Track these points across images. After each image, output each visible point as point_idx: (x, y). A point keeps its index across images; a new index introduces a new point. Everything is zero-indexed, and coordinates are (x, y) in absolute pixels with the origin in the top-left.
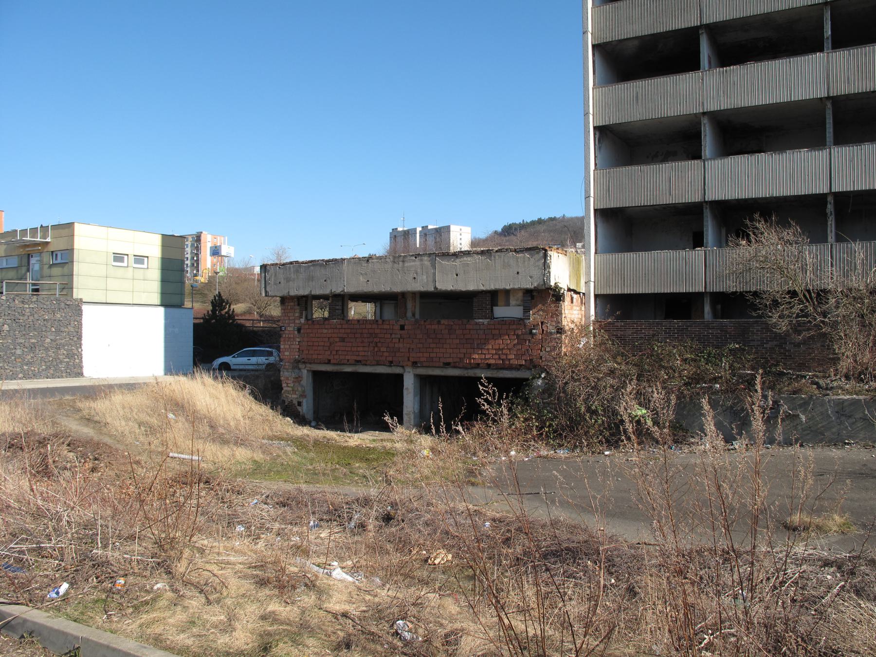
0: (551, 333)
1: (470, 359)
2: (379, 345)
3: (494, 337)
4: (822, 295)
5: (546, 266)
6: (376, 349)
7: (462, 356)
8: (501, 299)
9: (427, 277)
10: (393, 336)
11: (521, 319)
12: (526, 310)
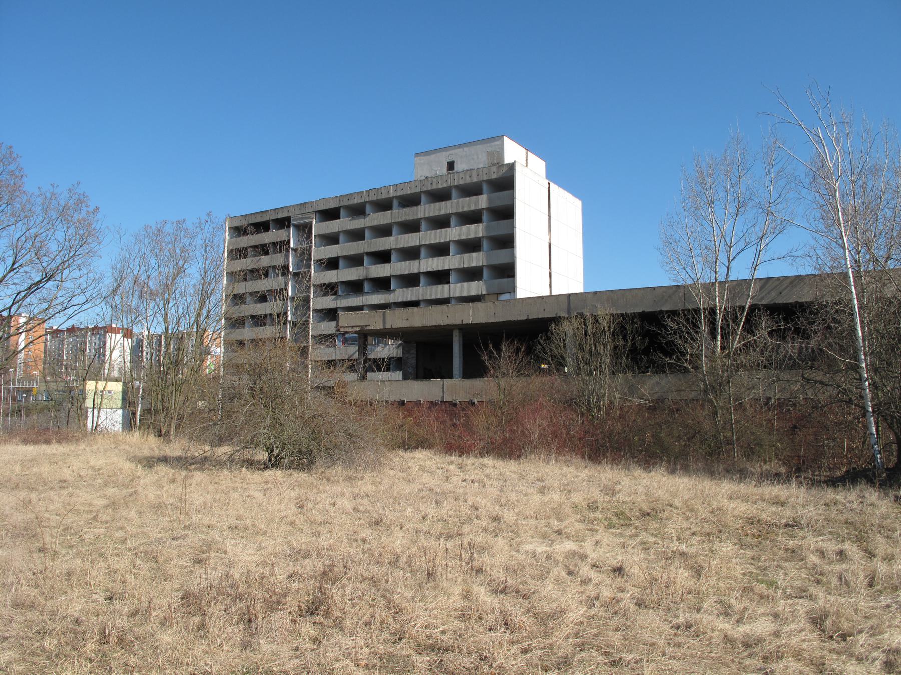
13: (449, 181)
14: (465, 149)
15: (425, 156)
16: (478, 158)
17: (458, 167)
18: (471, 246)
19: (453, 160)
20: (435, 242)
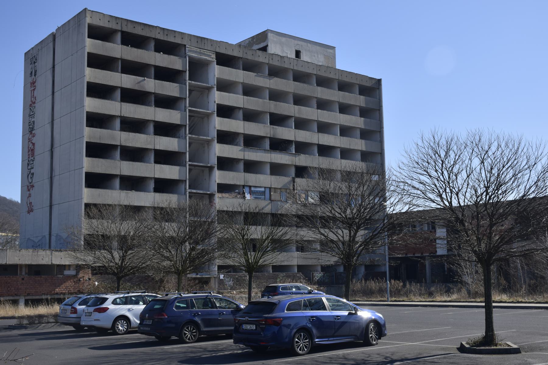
0: (87, 280)
1: (54, 291)
2: (10, 287)
3: (65, 282)
6: (9, 289)
7: (51, 290)
8: (67, 268)
9: (48, 259)
10: (18, 283)
11: (75, 275)
14: (309, 45)
15: (276, 35)
16: (318, 57)
17: (305, 57)
18: (345, 131)
19: (300, 50)
20: (325, 121)
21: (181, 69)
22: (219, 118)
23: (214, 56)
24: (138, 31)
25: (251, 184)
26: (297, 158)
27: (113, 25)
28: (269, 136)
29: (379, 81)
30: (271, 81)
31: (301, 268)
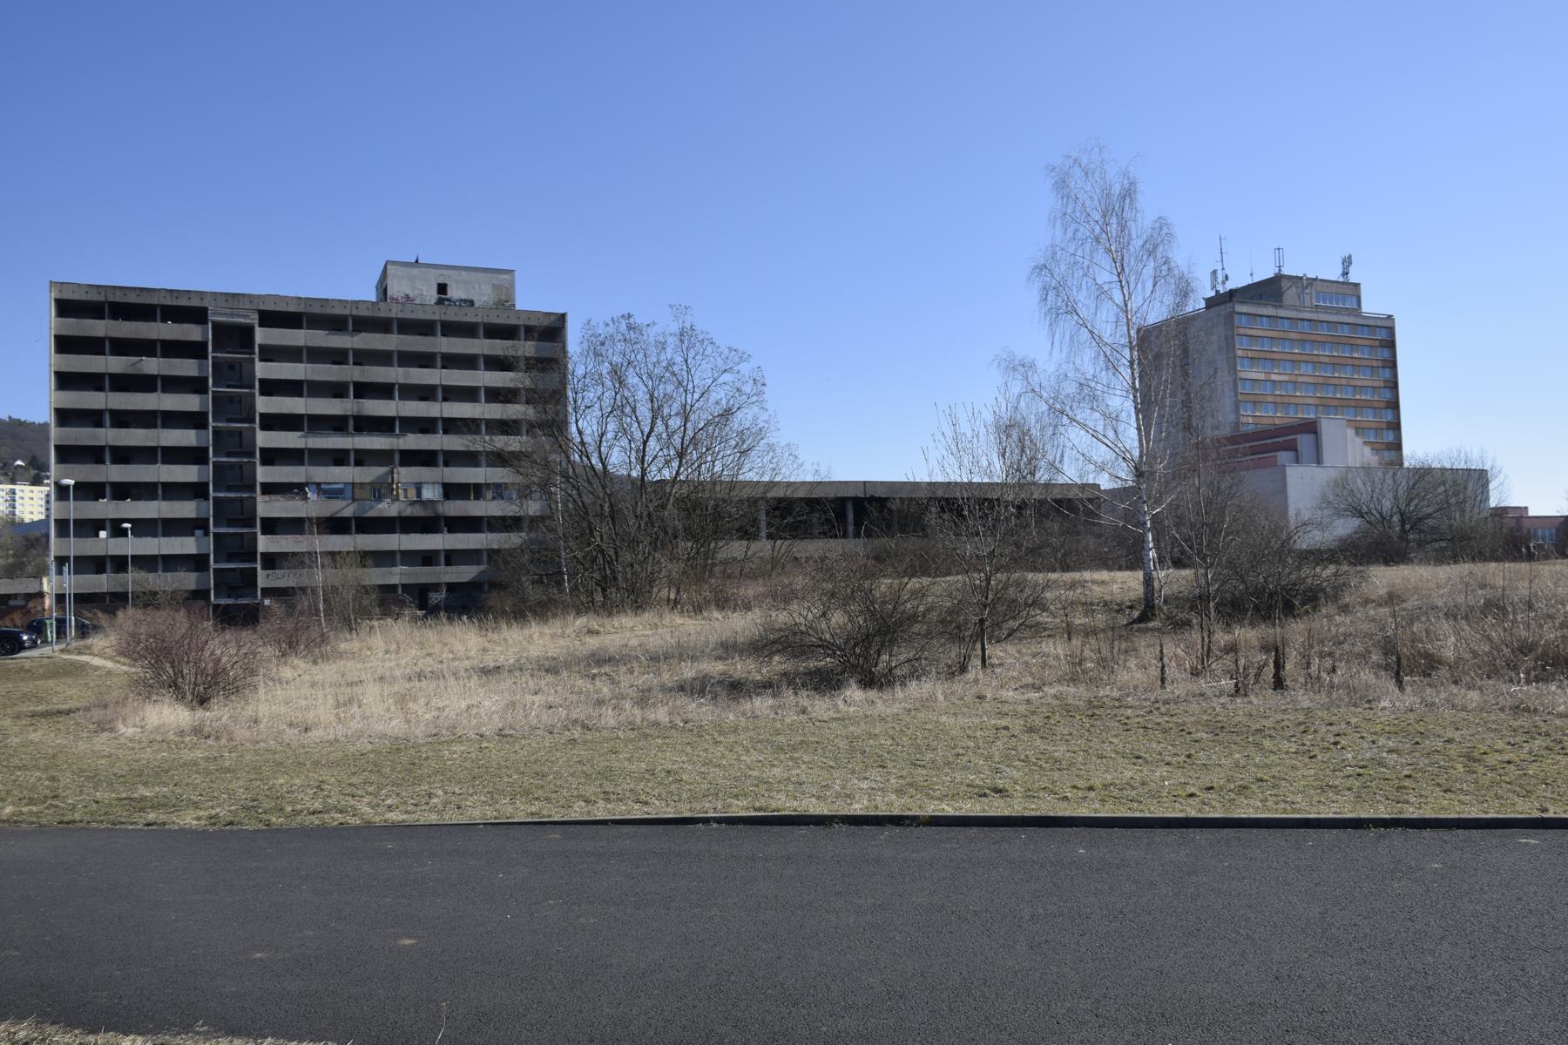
4: (155, 593)
5: (41, 584)
12: (27, 602)
13: (480, 315)
14: (463, 273)
16: (480, 289)
17: (454, 293)
21: (199, 339)
22: (264, 398)
23: (256, 316)
24: (132, 299)
25: (317, 480)
26: (401, 440)
27: (93, 297)
28: (349, 413)
29: (563, 316)
30: (356, 338)
31: (406, 588)
